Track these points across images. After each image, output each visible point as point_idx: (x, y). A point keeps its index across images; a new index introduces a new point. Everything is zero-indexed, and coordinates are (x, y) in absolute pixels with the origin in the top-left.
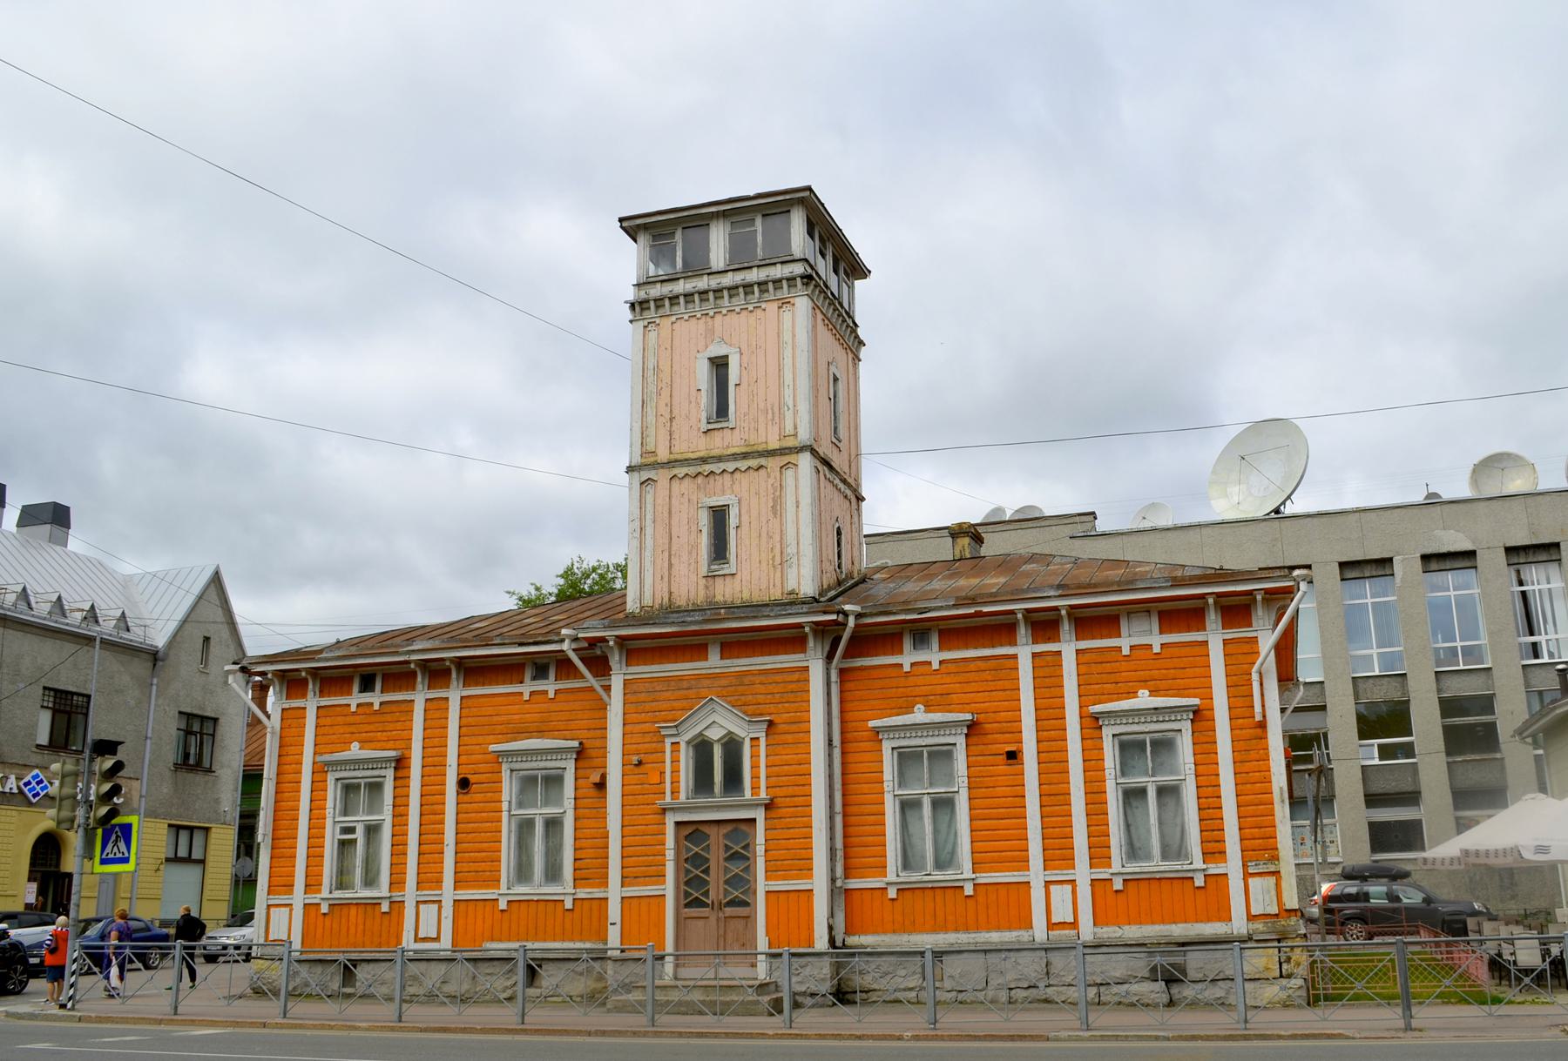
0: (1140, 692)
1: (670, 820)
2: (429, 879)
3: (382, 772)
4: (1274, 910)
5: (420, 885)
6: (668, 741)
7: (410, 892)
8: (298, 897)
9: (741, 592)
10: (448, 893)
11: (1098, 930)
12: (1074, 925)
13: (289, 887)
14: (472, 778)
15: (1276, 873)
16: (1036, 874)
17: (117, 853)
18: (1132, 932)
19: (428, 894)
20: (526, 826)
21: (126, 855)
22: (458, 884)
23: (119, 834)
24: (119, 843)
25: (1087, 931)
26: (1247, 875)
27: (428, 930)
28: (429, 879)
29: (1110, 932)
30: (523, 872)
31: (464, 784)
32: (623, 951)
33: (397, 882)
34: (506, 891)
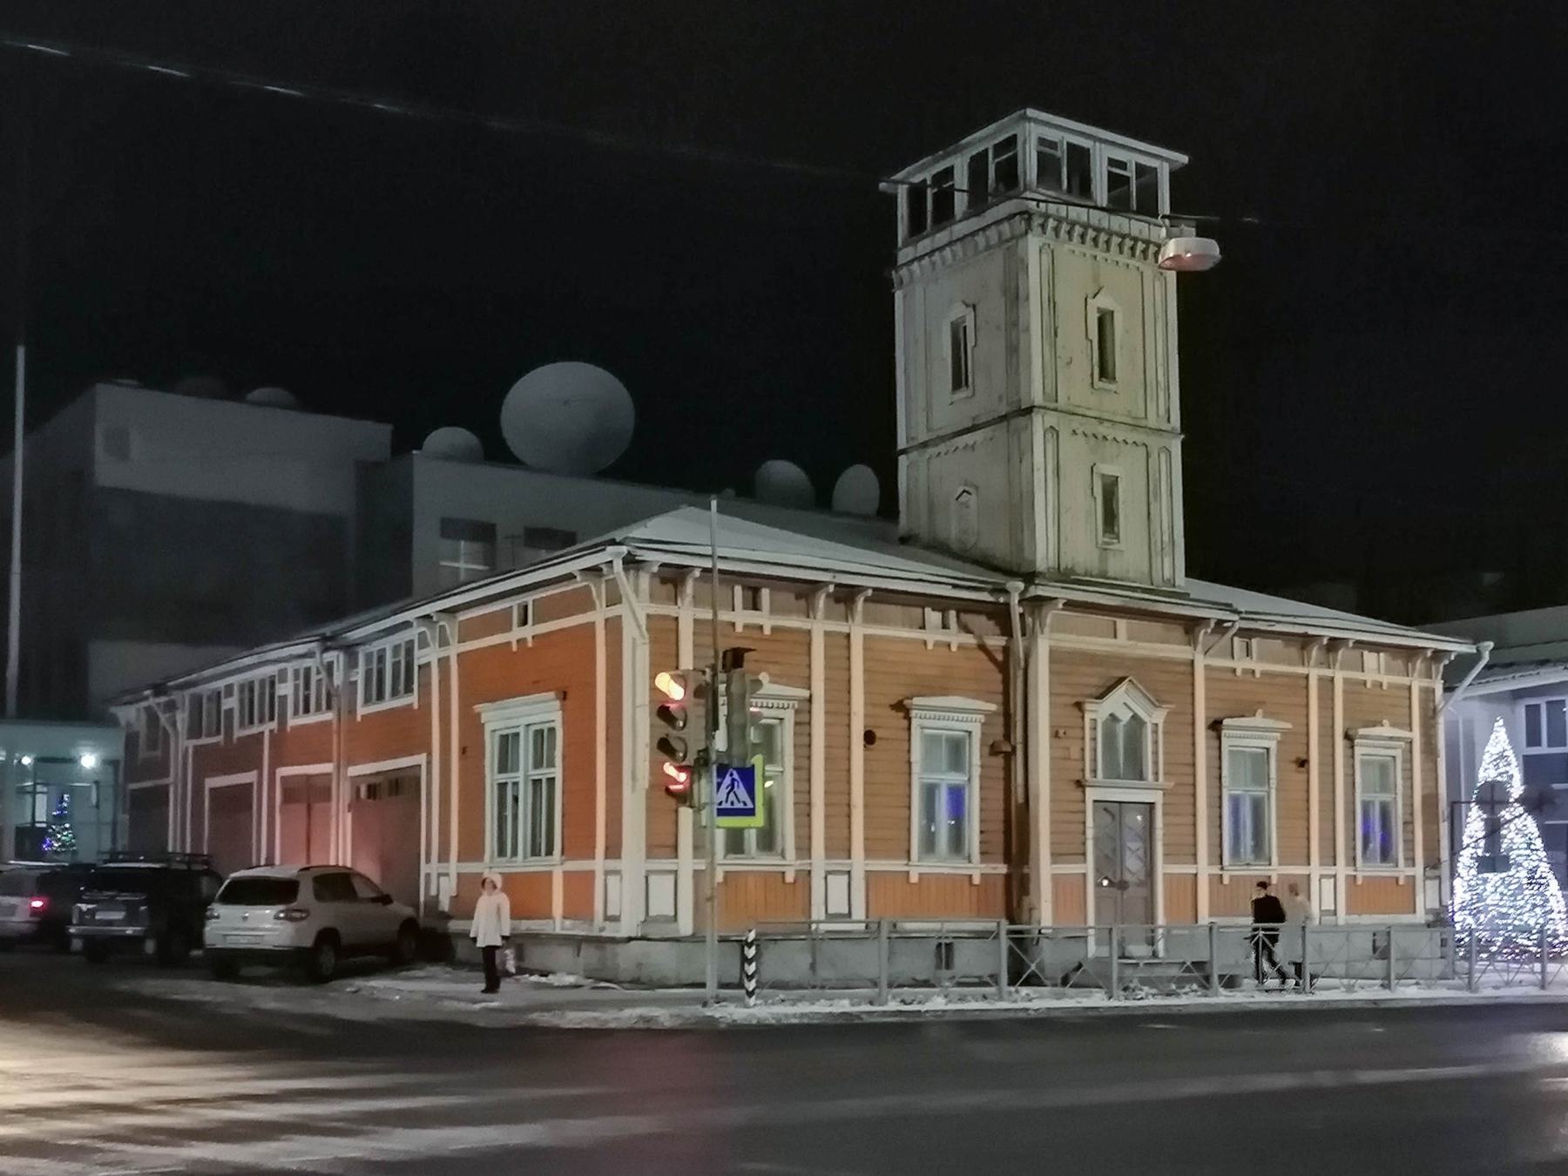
0: (1384, 721)
1: (1092, 794)
2: (839, 847)
3: (780, 713)
4: (1437, 906)
5: (830, 852)
6: (1088, 716)
7: (819, 861)
8: (687, 862)
9: (1128, 571)
10: (859, 862)
11: (1348, 917)
12: (1335, 913)
13: (674, 850)
14: (879, 733)
15: (1439, 878)
16: (1315, 869)
17: (736, 801)
18: (1367, 919)
19: (839, 864)
20: (930, 792)
21: (750, 805)
22: (869, 852)
23: (736, 776)
24: (735, 789)
25: (1342, 918)
26: (1426, 878)
27: (838, 906)
28: (839, 847)
29: (1355, 919)
30: (929, 844)
31: (869, 738)
32: (1054, 929)
33: (804, 849)
34: (918, 867)
